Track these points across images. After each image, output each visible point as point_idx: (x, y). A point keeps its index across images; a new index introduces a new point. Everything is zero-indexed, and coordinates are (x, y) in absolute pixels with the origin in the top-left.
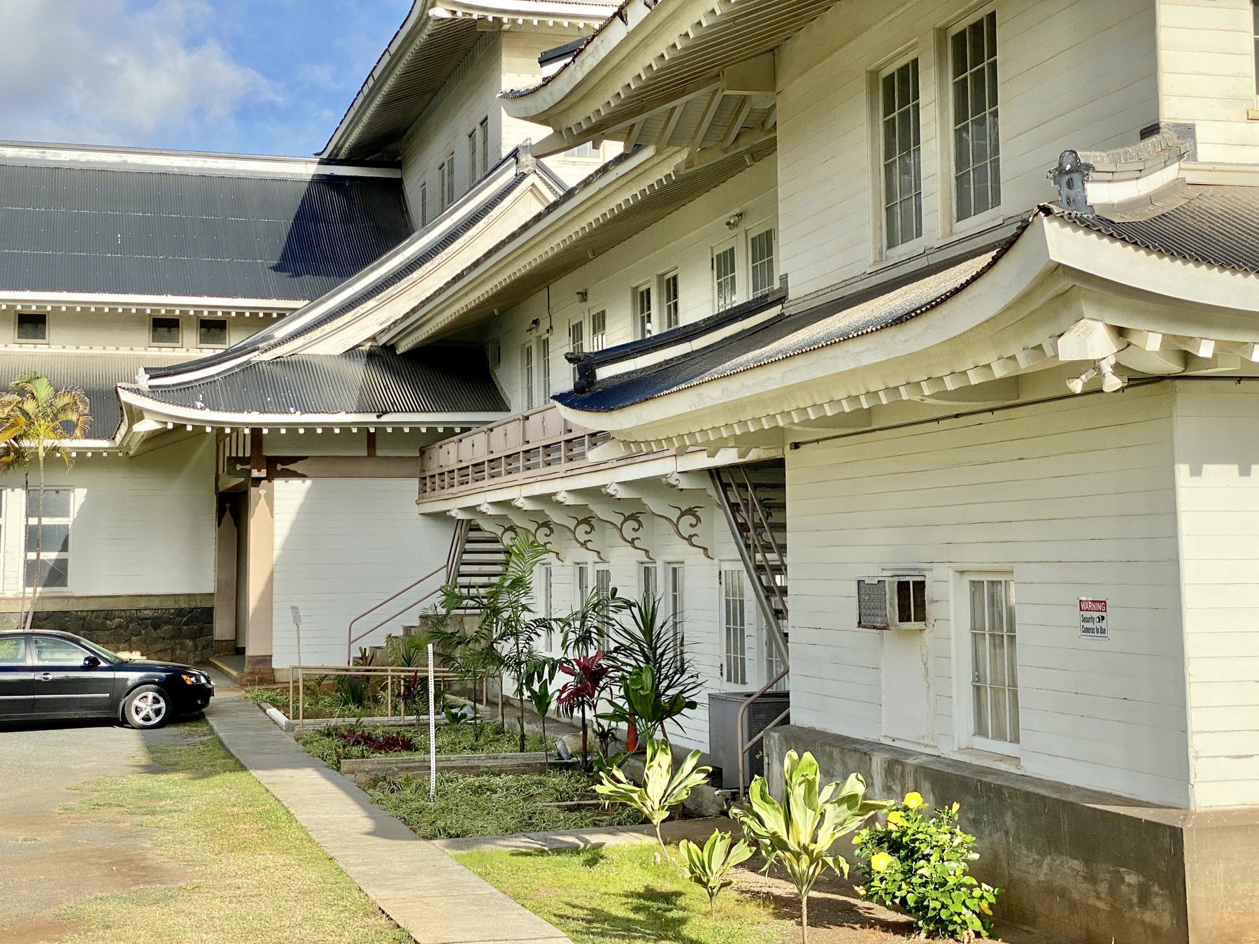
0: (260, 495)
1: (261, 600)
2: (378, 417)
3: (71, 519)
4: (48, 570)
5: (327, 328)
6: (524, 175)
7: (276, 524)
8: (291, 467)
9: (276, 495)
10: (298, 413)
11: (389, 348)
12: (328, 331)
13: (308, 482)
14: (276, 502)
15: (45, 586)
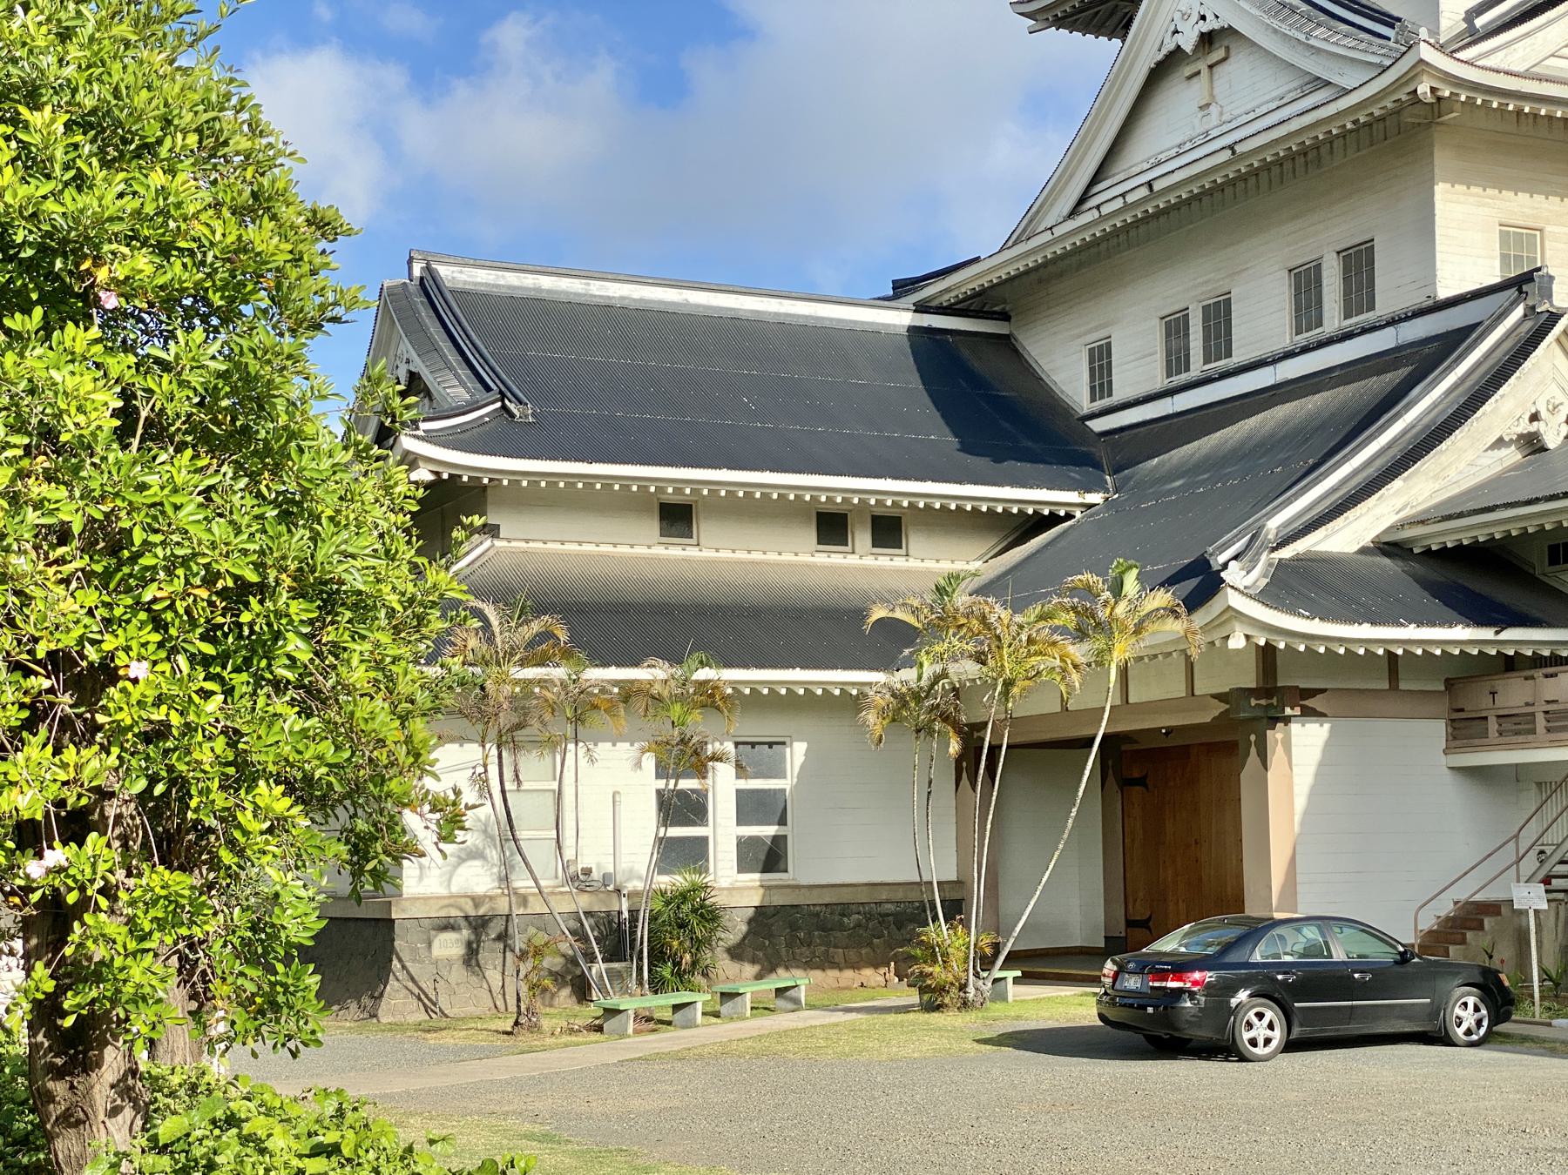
0: (1276, 741)
1: (1284, 886)
2: (1497, 633)
3: (789, 781)
4: (766, 849)
5: (1350, 514)
6: (1554, 318)
7: (1296, 780)
8: (1309, 703)
9: (1294, 740)
10: (1413, 626)
11: (1395, 544)
12: (1351, 519)
13: (1327, 726)
14: (1294, 750)
15: (765, 870)
